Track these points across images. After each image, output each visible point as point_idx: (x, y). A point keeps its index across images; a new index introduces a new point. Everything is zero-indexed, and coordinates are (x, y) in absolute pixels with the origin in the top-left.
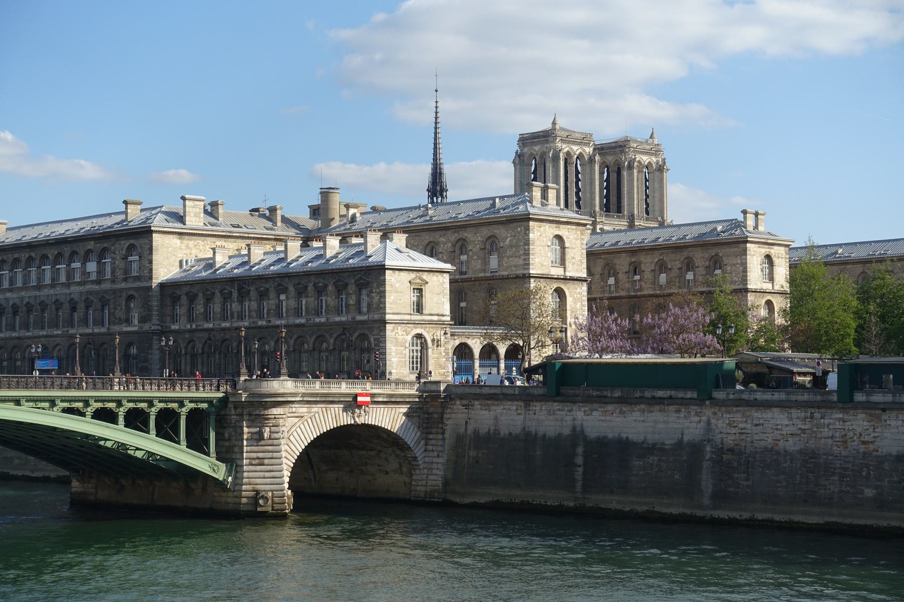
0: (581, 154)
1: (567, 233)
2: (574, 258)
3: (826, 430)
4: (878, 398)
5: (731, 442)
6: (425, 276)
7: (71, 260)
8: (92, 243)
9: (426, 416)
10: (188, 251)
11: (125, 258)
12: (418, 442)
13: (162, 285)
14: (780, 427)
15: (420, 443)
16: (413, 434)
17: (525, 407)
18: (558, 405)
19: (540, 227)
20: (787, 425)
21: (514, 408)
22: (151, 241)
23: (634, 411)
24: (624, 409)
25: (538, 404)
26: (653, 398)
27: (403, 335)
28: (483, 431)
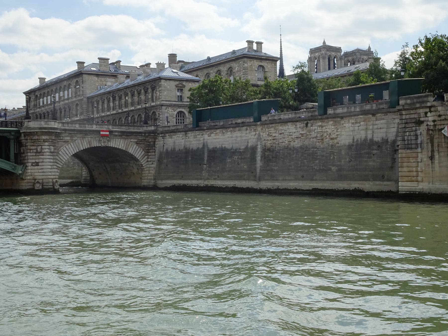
0: (336, 56)
1: (266, 65)
2: (271, 77)
3: (313, 133)
4: (340, 110)
5: (269, 145)
6: (184, 83)
7: (60, 91)
8: (66, 82)
9: (148, 143)
10: (101, 83)
11: (75, 87)
12: (143, 156)
13: (88, 98)
14: (291, 134)
15: (144, 157)
16: (140, 153)
17: (185, 135)
18: (198, 132)
19: (251, 61)
20: (295, 132)
21: (181, 136)
22: (83, 78)
23: (228, 132)
24: (224, 131)
25: (190, 133)
26: (236, 123)
27: (172, 111)
28: (169, 149)
